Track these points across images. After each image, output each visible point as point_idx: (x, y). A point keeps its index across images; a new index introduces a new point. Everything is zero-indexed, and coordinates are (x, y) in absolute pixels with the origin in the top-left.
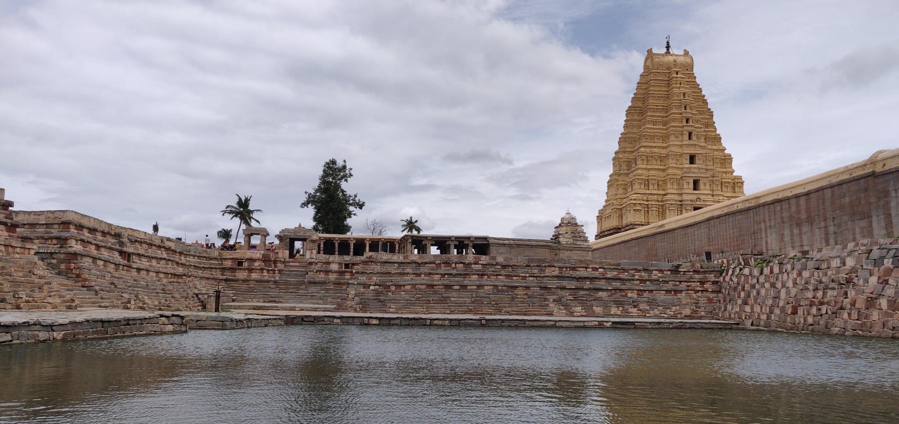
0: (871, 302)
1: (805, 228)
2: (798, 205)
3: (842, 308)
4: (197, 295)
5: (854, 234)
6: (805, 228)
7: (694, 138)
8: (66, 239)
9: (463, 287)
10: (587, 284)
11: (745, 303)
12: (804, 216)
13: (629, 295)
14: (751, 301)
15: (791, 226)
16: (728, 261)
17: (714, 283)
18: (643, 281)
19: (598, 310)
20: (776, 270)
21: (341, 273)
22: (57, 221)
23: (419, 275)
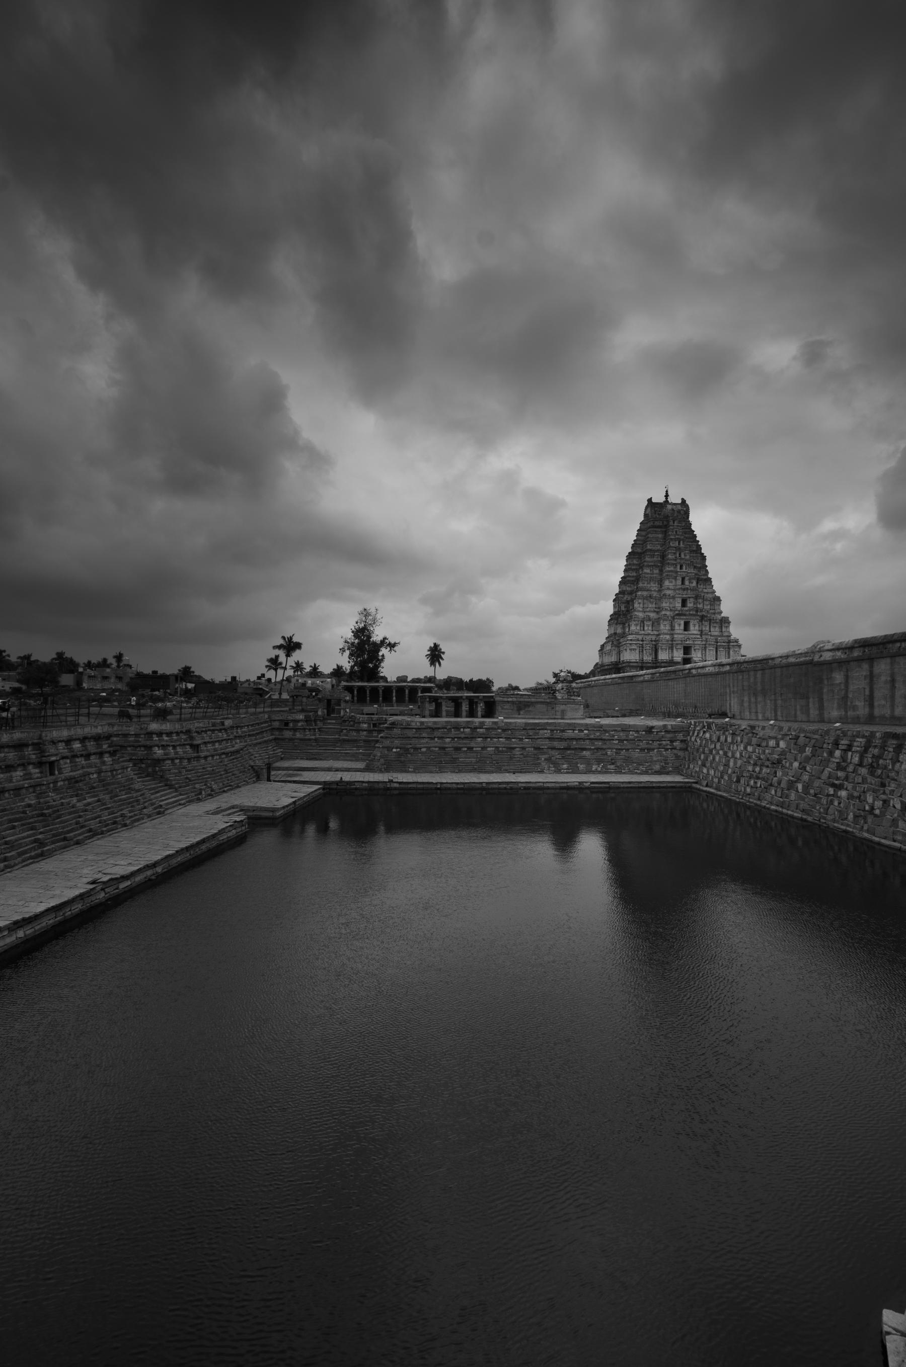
0: (791, 785)
1: (760, 699)
2: (755, 678)
3: (771, 785)
4: (252, 767)
5: (796, 710)
6: (760, 699)
7: (687, 583)
8: (151, 747)
9: (470, 749)
11: (704, 765)
12: (759, 687)
14: (708, 765)
17: (682, 741)
18: (621, 741)
19: (581, 767)
20: (729, 739)
21: (370, 731)
22: (143, 732)
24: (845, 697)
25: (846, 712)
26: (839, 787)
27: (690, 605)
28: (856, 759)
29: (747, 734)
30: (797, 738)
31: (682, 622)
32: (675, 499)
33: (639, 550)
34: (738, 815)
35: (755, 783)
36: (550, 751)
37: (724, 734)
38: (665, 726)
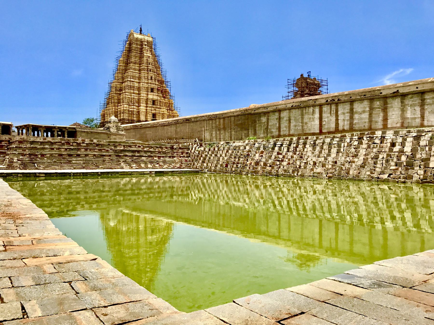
0: (257, 163)
2: (220, 122)
3: (246, 165)
5: (242, 136)
10: (137, 154)
11: (203, 162)
14: (206, 161)
15: (216, 130)
16: (192, 144)
18: (159, 152)
19: (143, 165)
20: (216, 149)
23: (53, 149)
24: (267, 128)
26: (282, 161)
28: (286, 150)
34: (227, 182)
36: (125, 158)
37: (212, 147)
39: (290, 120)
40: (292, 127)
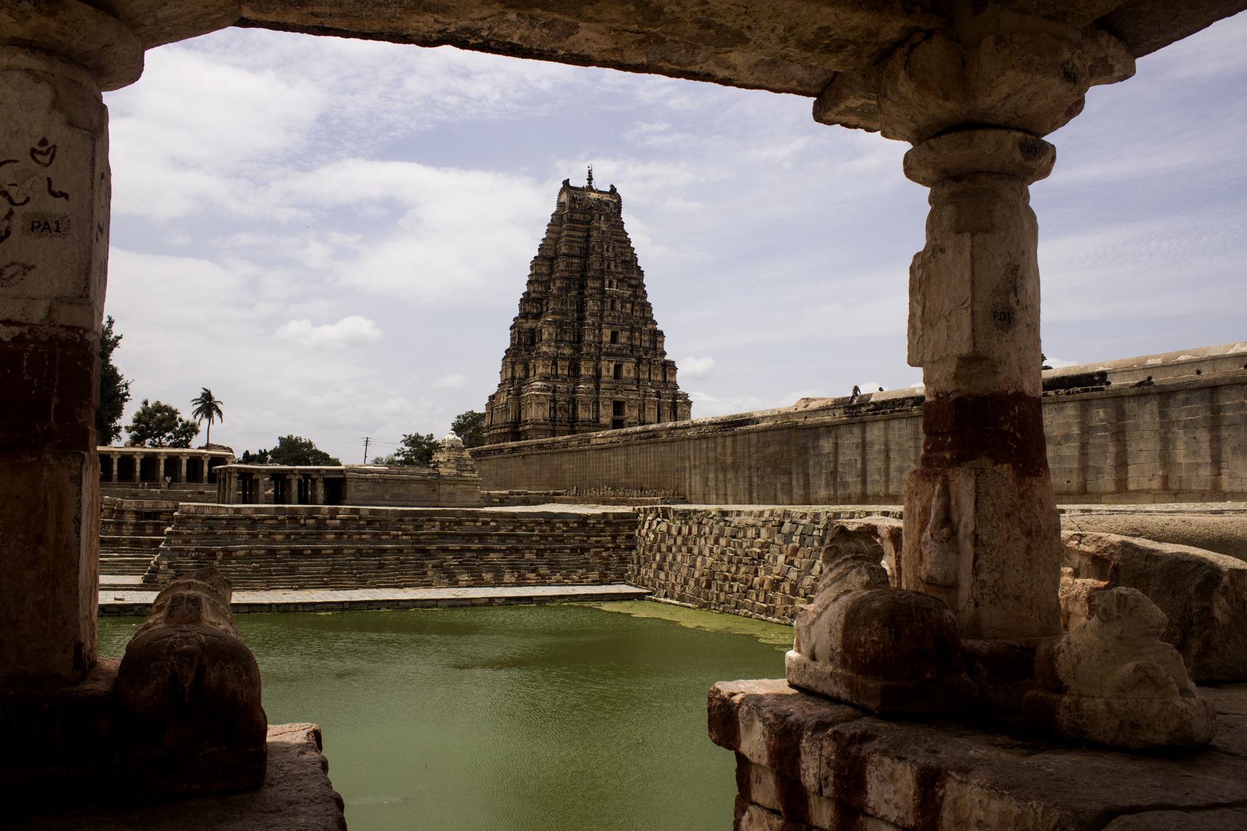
1: (730, 475)
2: (724, 446)
3: (751, 588)
6: (730, 475)
11: (660, 568)
12: (729, 460)
13: (527, 556)
14: (667, 568)
15: (716, 470)
19: (488, 576)
24: (834, 472)
25: (836, 491)
27: (623, 338)
29: (718, 523)
30: (781, 524)
31: (612, 366)
32: (601, 184)
33: (551, 253)
35: (731, 587)
37: (686, 523)
38: (605, 514)
39: (887, 451)
40: (893, 474)
